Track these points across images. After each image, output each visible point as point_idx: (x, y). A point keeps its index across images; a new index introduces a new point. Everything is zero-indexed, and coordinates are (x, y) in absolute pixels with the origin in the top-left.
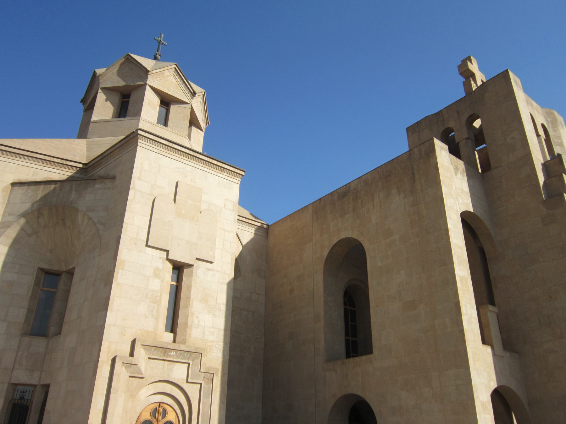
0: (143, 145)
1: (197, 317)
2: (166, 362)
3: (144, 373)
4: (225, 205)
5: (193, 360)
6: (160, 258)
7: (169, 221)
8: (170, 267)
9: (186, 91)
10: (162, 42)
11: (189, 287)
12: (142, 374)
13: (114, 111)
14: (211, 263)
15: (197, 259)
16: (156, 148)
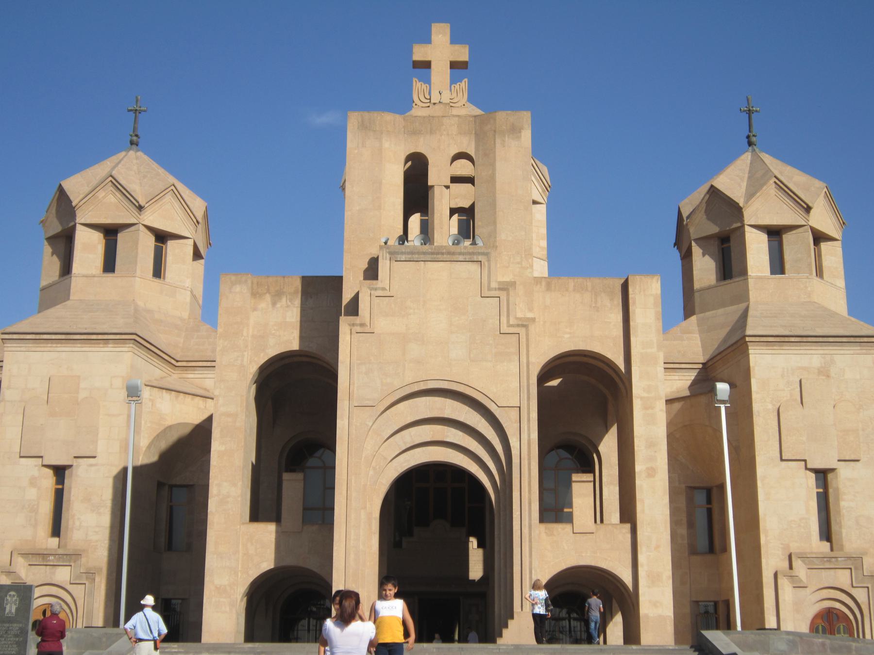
0: (10, 349)
1: (79, 519)
2: (48, 567)
3: (25, 579)
4: (111, 385)
5: (75, 562)
6: (36, 466)
7: (42, 425)
8: (50, 472)
9: (130, 207)
10: (140, 110)
11: (70, 488)
12: (22, 579)
13: (61, 265)
14: (94, 457)
15: (75, 457)
16: (23, 346)
